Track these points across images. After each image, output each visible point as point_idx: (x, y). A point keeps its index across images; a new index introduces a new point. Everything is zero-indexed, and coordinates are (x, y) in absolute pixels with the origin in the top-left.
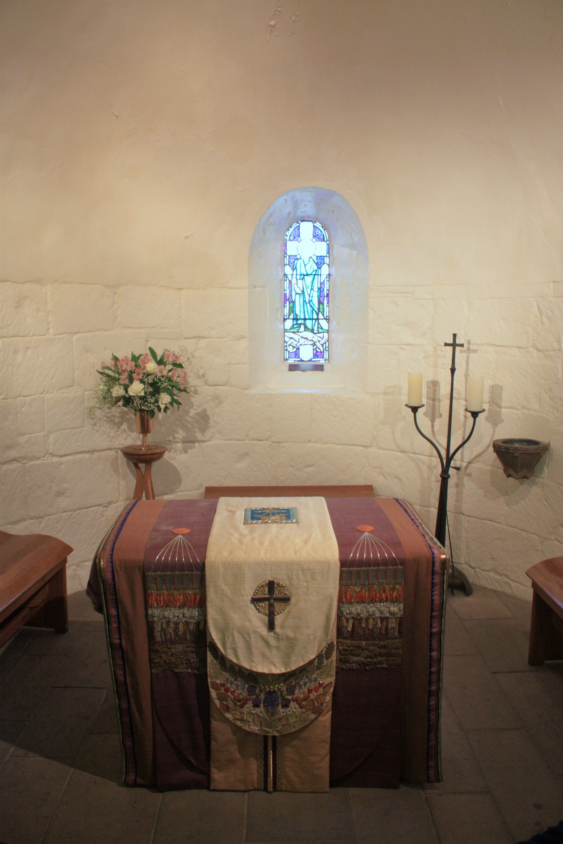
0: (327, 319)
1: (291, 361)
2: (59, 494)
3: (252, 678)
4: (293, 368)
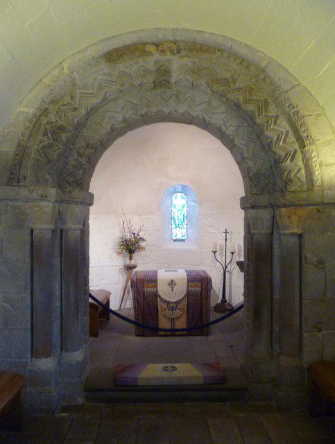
0: (187, 225)
1: (174, 238)
2: (102, 279)
3: (168, 303)
4: (175, 241)
